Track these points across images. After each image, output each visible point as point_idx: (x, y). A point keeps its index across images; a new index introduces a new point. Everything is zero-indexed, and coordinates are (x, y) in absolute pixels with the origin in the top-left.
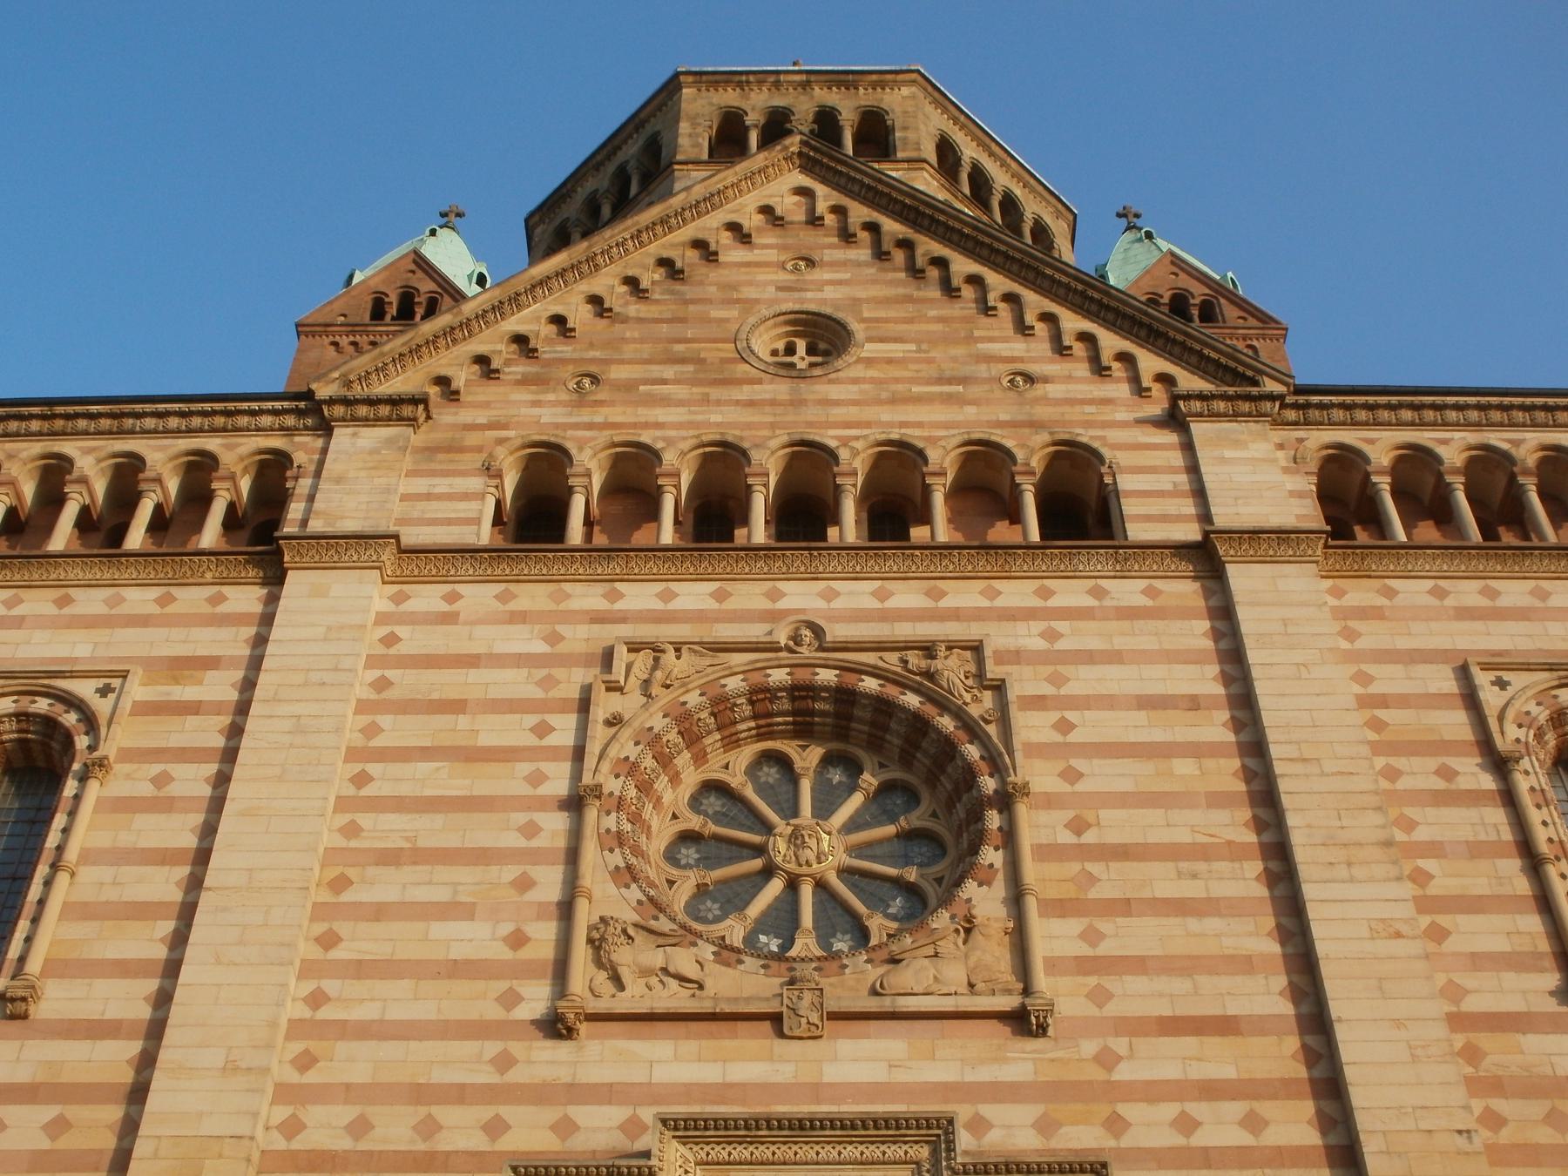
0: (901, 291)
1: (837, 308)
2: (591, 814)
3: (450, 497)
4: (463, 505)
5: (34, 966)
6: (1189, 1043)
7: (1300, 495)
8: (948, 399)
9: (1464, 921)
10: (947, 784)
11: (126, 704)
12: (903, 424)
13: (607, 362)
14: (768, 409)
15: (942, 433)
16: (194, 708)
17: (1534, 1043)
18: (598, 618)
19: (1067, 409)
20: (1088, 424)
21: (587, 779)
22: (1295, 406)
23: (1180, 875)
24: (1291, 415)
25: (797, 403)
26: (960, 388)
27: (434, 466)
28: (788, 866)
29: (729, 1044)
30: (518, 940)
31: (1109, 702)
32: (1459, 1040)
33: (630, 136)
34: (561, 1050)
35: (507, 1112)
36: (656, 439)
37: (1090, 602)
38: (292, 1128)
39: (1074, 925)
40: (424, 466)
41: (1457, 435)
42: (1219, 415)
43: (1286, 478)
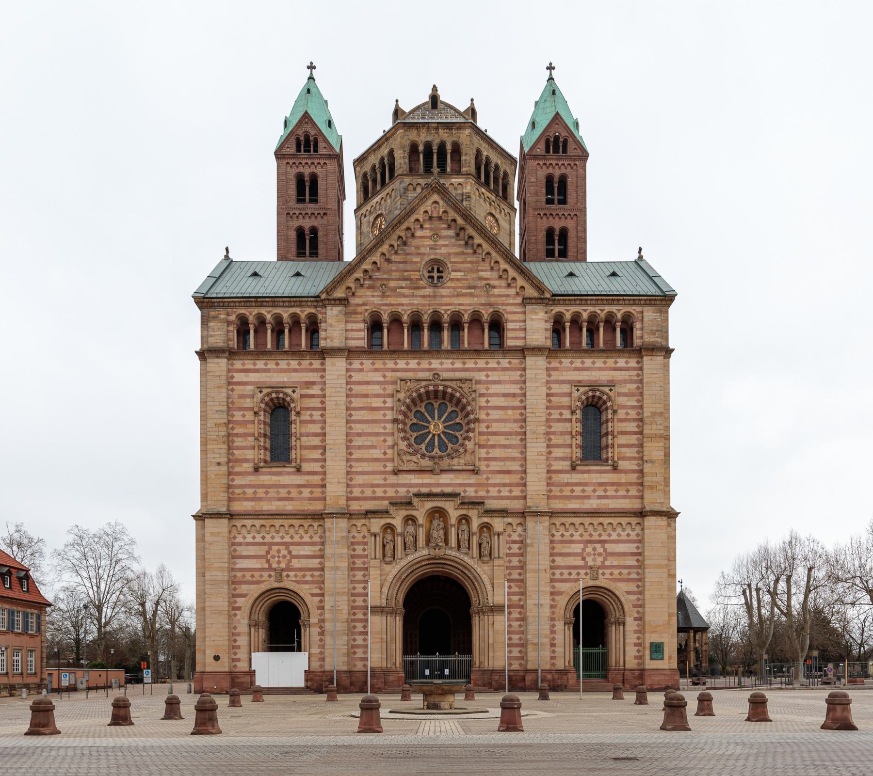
0: (461, 249)
4: (360, 333)
8: (471, 295)
9: (556, 450)
10: (464, 413)
12: (460, 305)
13: (388, 280)
14: (428, 299)
15: (468, 308)
16: (313, 396)
17: (562, 476)
18: (394, 370)
19: (498, 299)
20: (503, 304)
24: (550, 303)
25: (435, 296)
30: (385, 454)
34: (395, 477)
35: (387, 489)
36: (403, 310)
38: (351, 492)
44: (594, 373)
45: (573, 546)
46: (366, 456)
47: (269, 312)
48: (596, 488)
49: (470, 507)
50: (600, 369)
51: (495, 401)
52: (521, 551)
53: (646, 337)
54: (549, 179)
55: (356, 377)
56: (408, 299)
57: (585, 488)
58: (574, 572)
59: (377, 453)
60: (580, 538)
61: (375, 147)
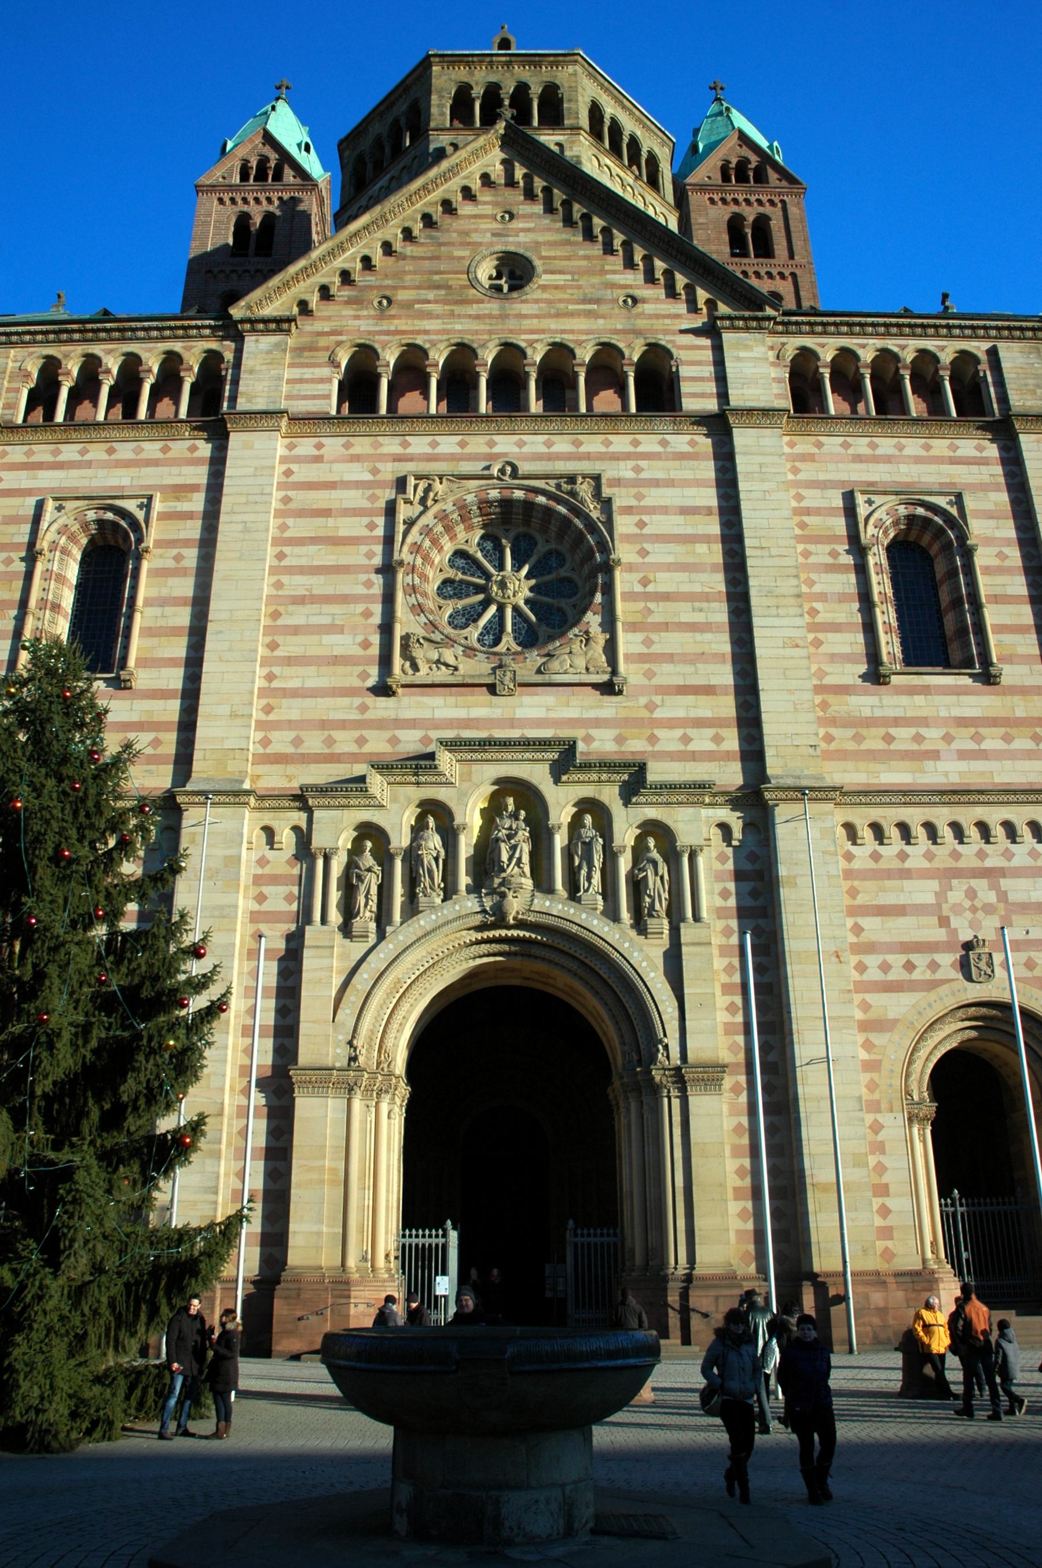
0: (564, 236)
1: (527, 249)
2: (400, 576)
3: (312, 381)
4: (320, 386)
5: (131, 662)
6: (690, 699)
7: (779, 380)
8: (589, 314)
9: (831, 637)
11: (154, 515)
12: (563, 332)
13: (395, 288)
14: (487, 321)
15: (584, 337)
17: (853, 700)
18: (398, 459)
19: (654, 321)
20: (666, 332)
21: (396, 556)
22: (782, 323)
23: (694, 610)
24: (780, 328)
25: (504, 317)
26: (595, 307)
27: (302, 360)
28: (499, 599)
29: (470, 698)
31: (664, 510)
32: (818, 699)
33: (400, 96)
35: (366, 733)
36: (425, 341)
37: (659, 449)
39: (639, 637)
40: (297, 361)
41: (871, 341)
42: (739, 328)
43: (772, 369)
44: (904, 468)
45: (907, 884)
46: (312, 652)
47: (109, 352)
48: (953, 731)
49: (604, 777)
50: (918, 460)
51: (657, 524)
52: (760, 902)
53: (1016, 397)
54: (735, 225)
55: (302, 473)
56: (439, 321)
57: (923, 731)
58: (920, 960)
59: (345, 644)
60: (926, 864)
61: (382, 108)
